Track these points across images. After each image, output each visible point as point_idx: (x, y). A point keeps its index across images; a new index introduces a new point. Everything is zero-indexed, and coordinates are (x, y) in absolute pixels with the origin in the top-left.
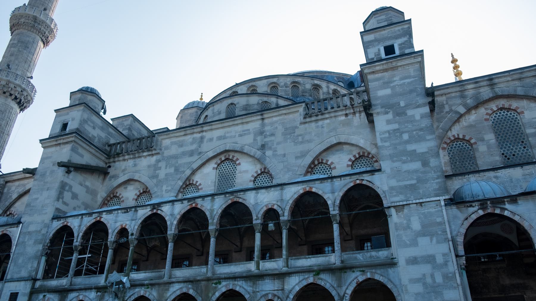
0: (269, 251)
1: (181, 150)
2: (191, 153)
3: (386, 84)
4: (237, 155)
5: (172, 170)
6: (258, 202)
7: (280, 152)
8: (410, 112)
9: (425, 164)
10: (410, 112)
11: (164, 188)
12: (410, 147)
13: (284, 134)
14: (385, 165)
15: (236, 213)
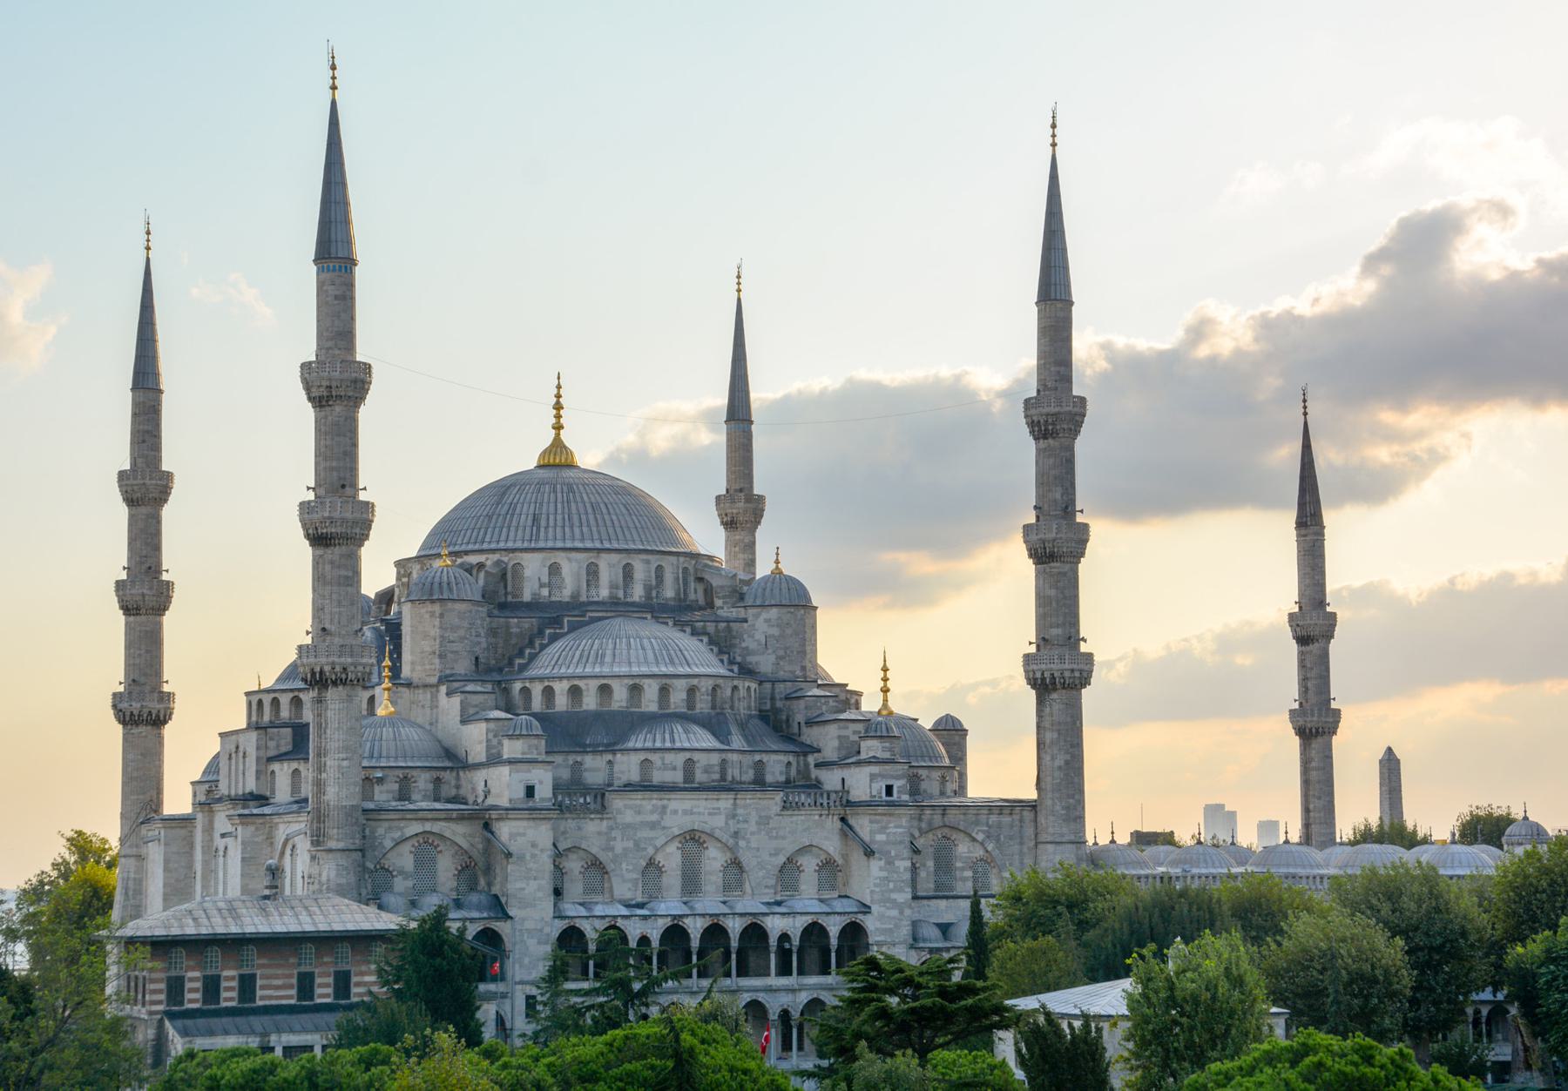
0: (784, 970)
1: (639, 819)
2: (653, 826)
3: (883, 830)
4: (704, 837)
5: (631, 844)
6: (775, 925)
7: (754, 845)
8: (897, 863)
9: (901, 913)
10: (897, 863)
11: (624, 866)
12: (894, 896)
13: (758, 823)
14: (875, 908)
15: (755, 933)
